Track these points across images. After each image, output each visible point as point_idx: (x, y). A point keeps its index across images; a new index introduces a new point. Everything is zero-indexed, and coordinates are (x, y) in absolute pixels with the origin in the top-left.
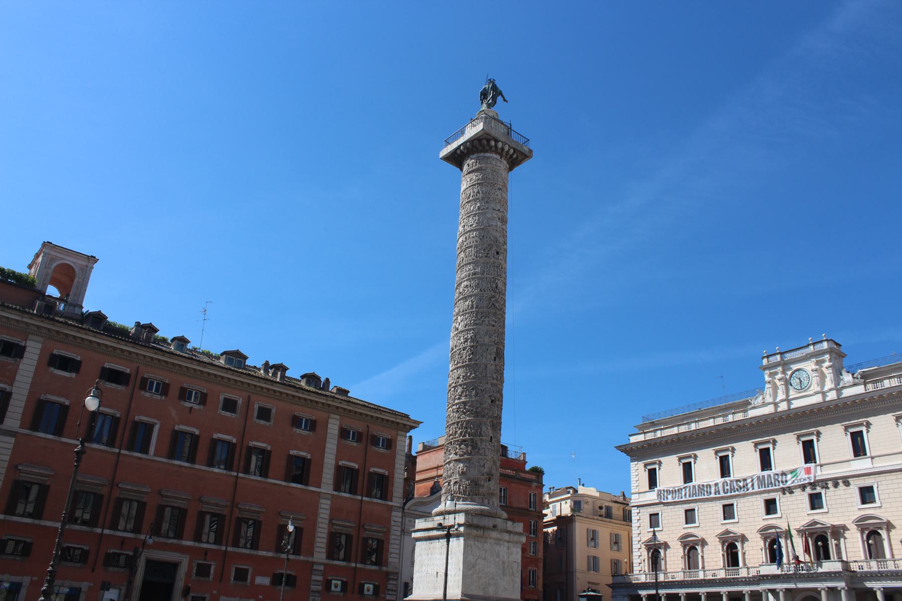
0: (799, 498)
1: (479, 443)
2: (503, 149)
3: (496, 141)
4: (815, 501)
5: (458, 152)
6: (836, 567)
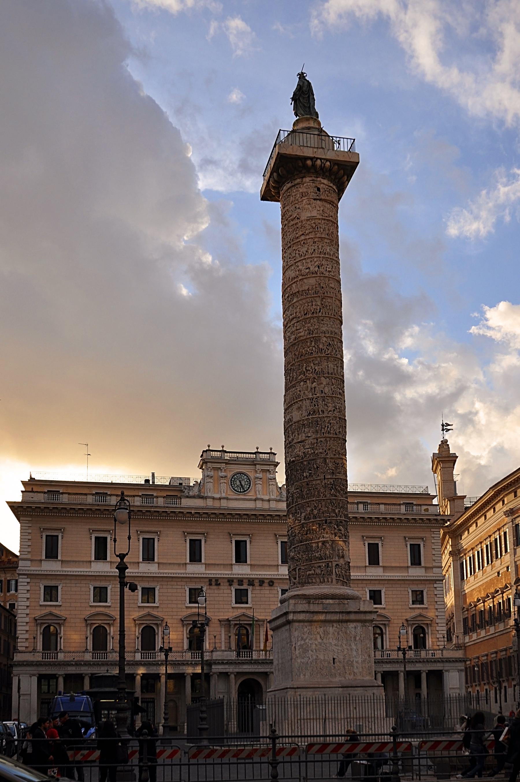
0: (225, 591)
4: (241, 597)
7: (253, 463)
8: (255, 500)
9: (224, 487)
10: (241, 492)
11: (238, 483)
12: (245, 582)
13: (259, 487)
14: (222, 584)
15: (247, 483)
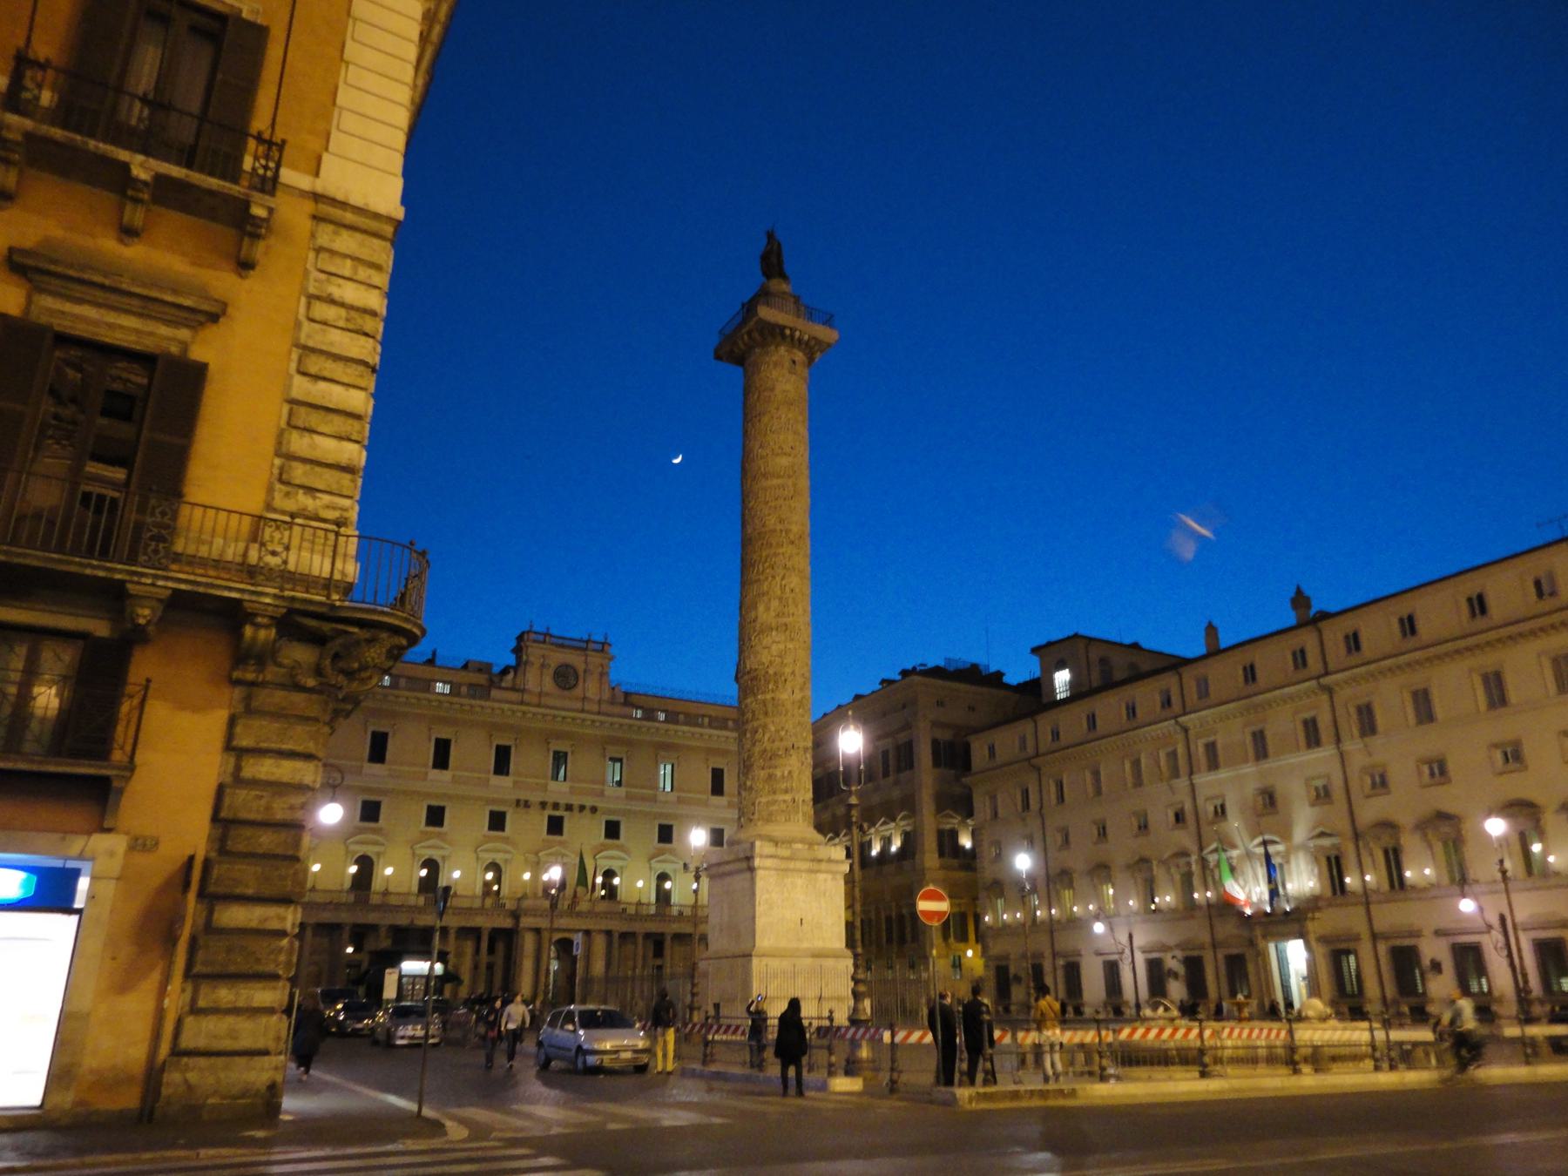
12: (562, 807)
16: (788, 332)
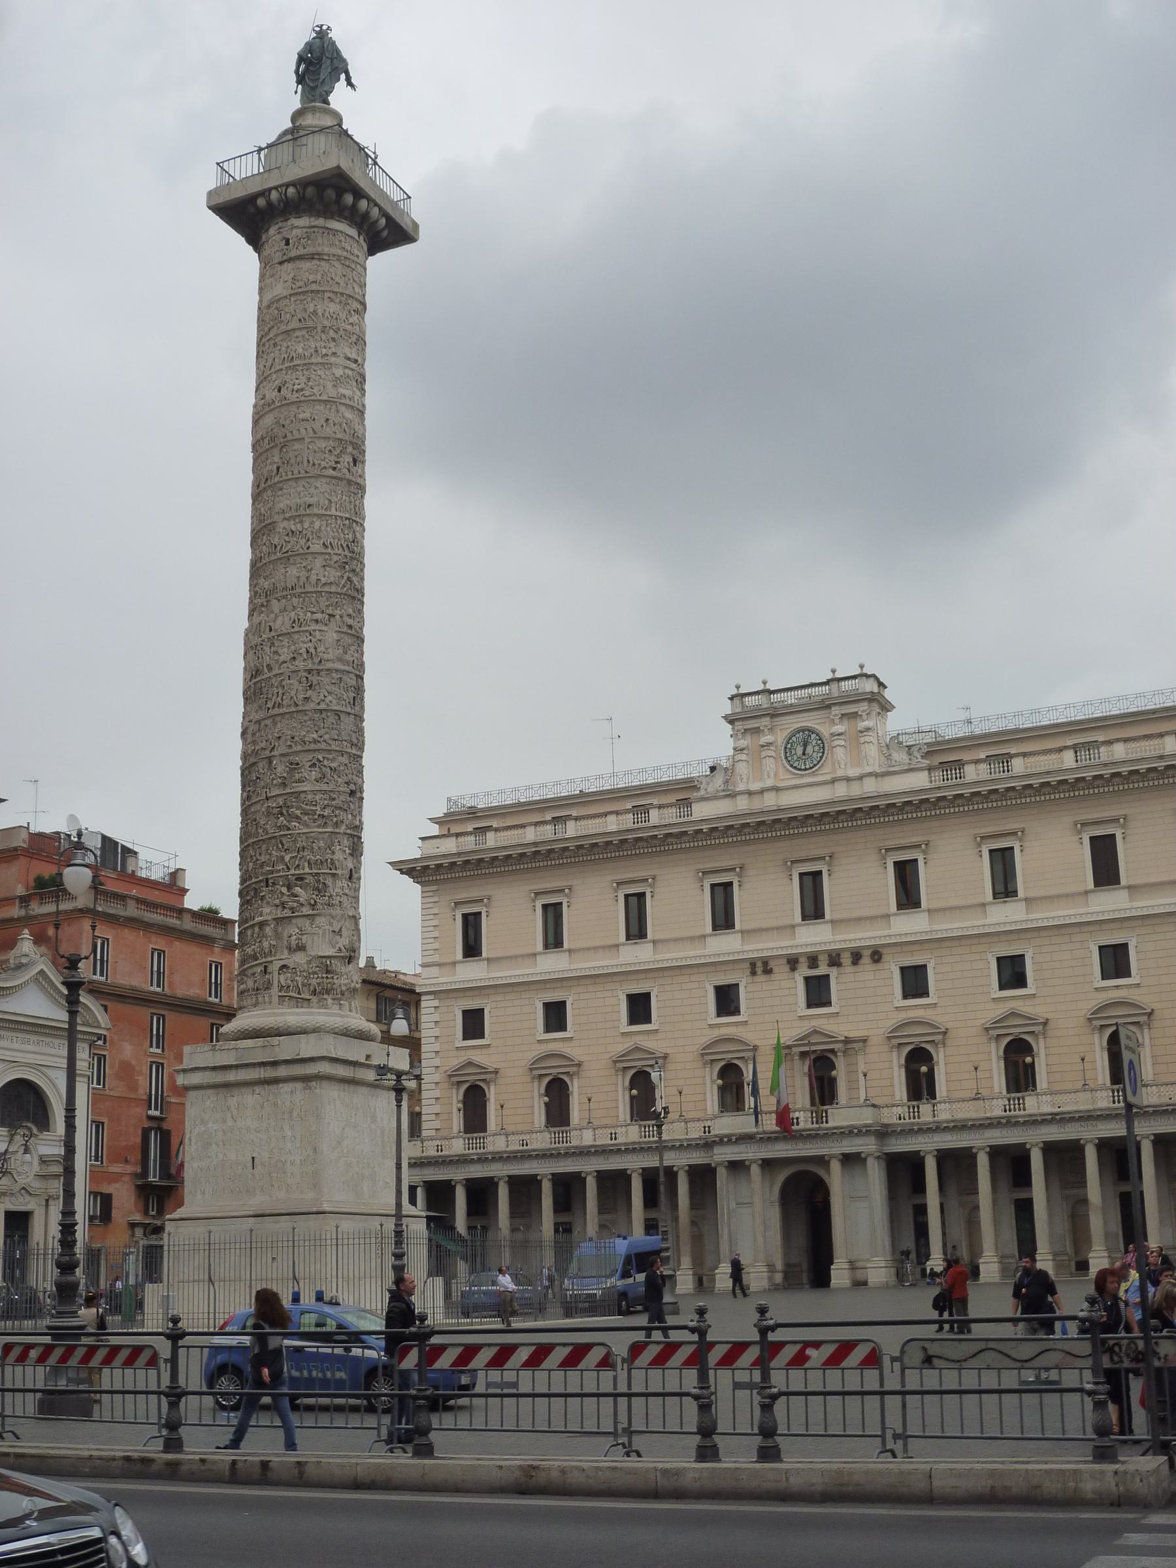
1: (329, 881)
2: (366, 216)
3: (359, 193)
4: (818, 991)
5: (261, 202)
6: (866, 1117)
7: (825, 705)
8: (833, 781)
9: (769, 765)
10: (806, 769)
11: (800, 750)
12: (823, 961)
13: (840, 753)
14: (775, 970)
15: (817, 748)
16: (261, 202)
